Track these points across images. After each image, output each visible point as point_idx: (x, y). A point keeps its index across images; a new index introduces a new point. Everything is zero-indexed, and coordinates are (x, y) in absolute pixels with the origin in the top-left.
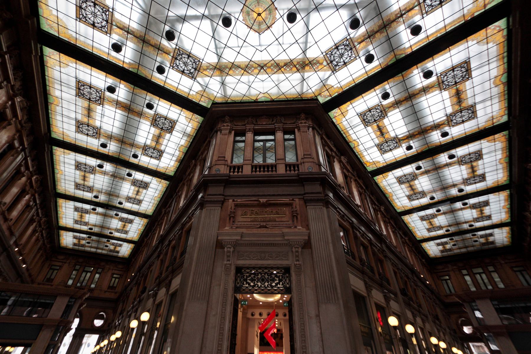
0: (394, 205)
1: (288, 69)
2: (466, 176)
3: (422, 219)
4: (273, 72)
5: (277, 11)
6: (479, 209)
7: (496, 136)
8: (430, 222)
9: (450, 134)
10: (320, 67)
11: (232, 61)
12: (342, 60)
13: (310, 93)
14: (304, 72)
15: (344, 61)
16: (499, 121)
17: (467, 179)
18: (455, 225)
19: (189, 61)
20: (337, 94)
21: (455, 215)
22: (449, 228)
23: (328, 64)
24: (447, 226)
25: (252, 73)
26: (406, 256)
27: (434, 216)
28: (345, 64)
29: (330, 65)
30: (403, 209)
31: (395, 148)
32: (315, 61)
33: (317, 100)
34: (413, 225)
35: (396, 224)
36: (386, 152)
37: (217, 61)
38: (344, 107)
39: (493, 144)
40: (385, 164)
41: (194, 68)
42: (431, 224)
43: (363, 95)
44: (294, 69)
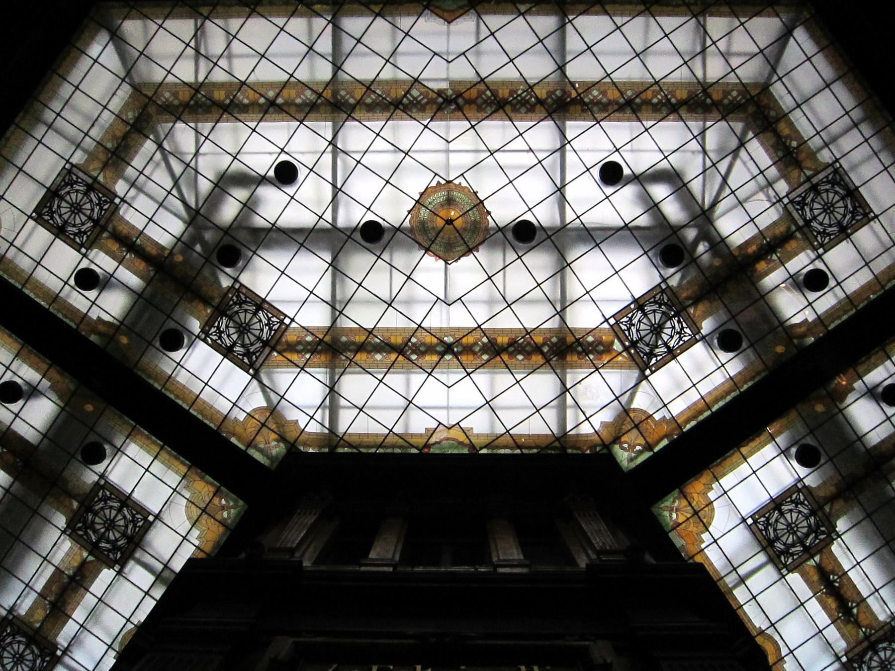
1: (520, 357)
4: (478, 362)
5: (489, 218)
11: (369, 325)
12: (660, 342)
13: (587, 435)
14: (564, 368)
15: (666, 344)
20: (665, 442)
23: (626, 349)
25: (420, 362)
28: (672, 354)
29: (633, 351)
32: (590, 339)
33: (611, 459)
37: (329, 325)
38: (695, 488)
41: (260, 342)
43: (744, 450)
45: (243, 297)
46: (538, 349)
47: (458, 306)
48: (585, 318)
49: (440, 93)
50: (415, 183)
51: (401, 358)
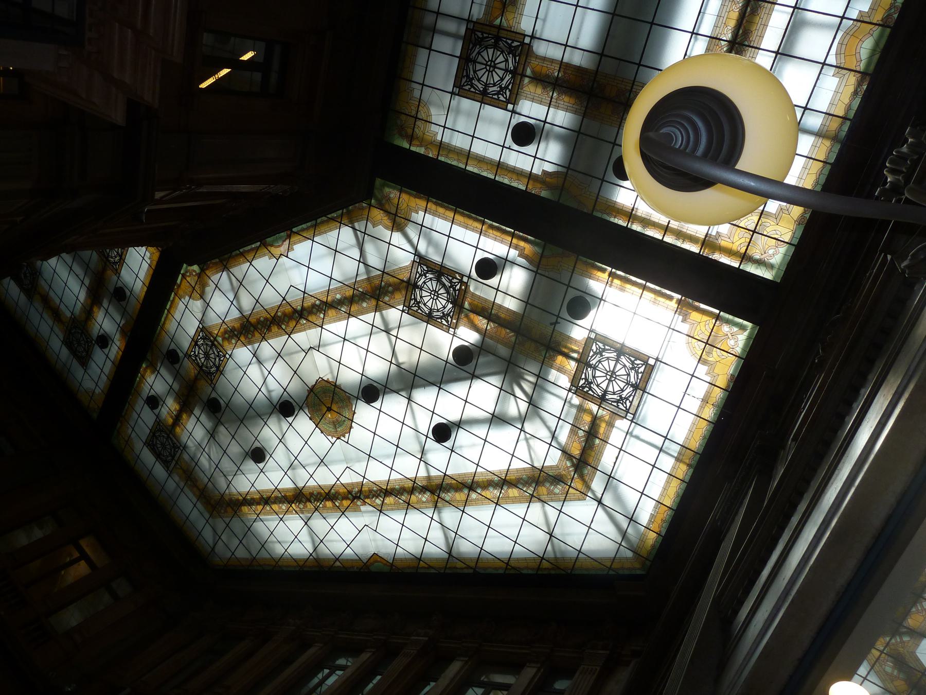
4: (281, 309)
10: (222, 330)
11: (352, 320)
19: (429, 304)
20: (178, 282)
23: (215, 339)
32: (233, 341)
44: (253, 320)
45: (444, 322)
46: (256, 328)
47: (306, 347)
48: (242, 354)
49: (365, 503)
50: (358, 435)
51: (325, 299)
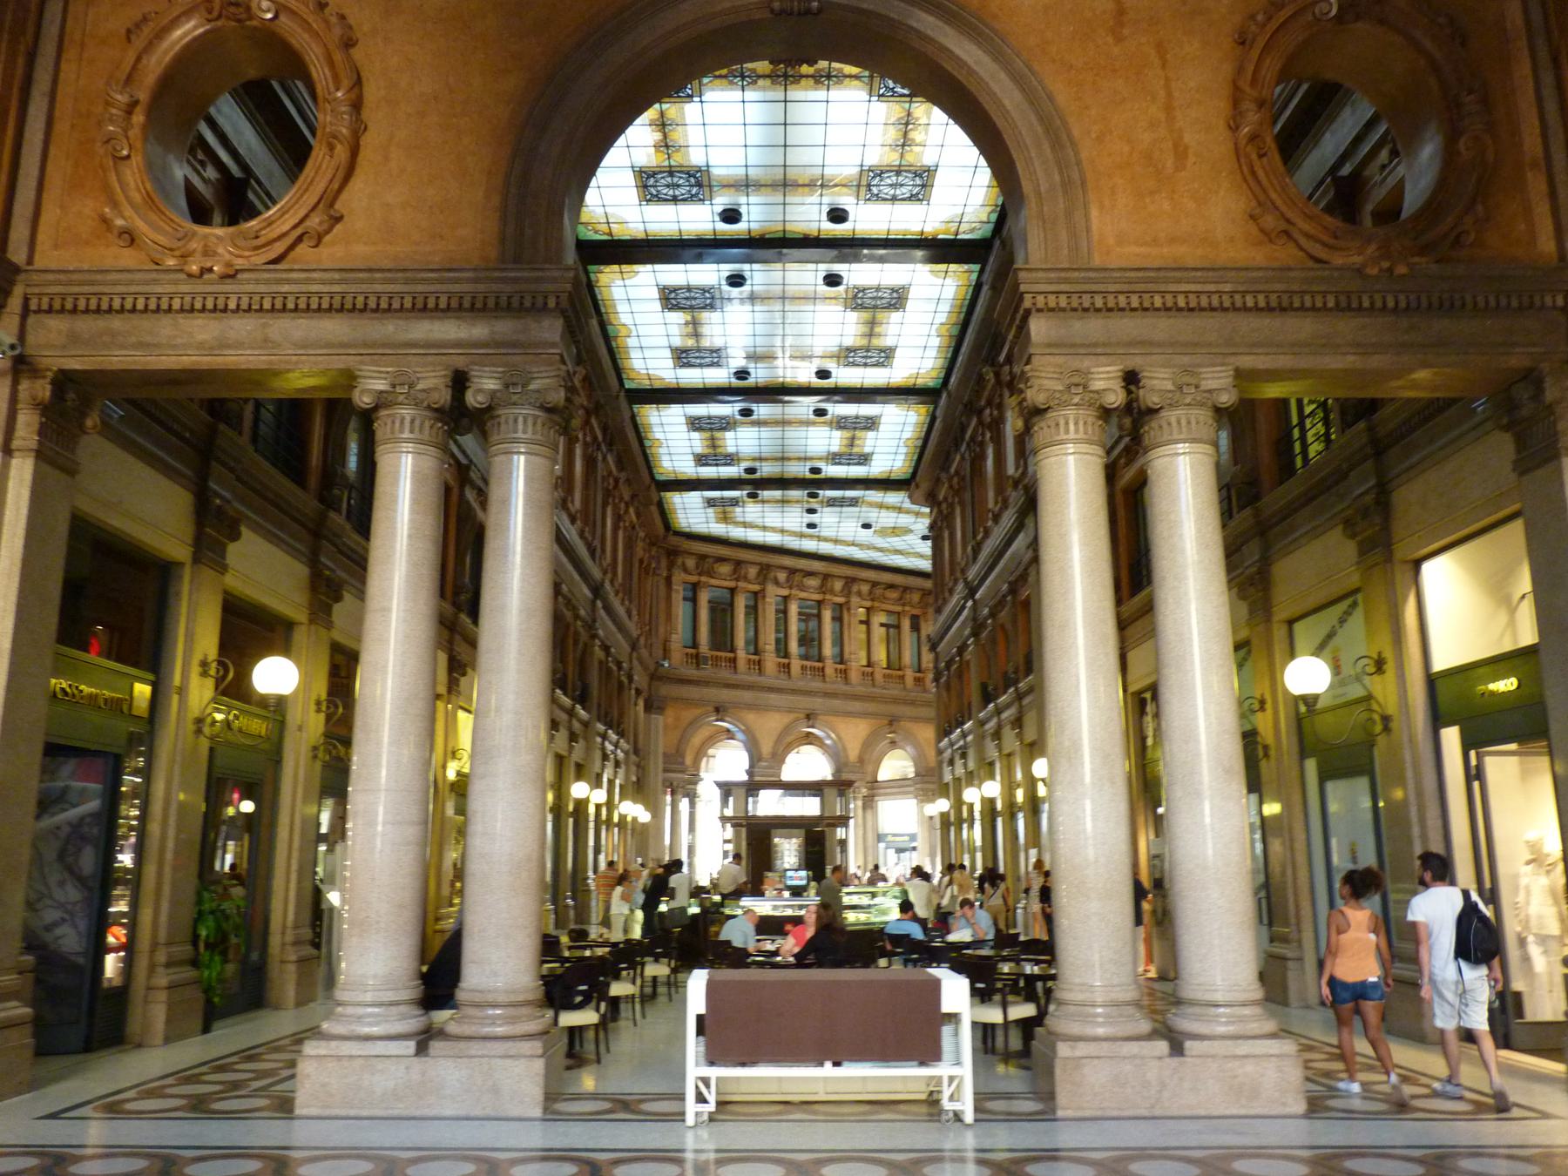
0: (624, 364)
2: (849, 342)
3: (695, 424)
6: (847, 434)
7: (953, 267)
8: (713, 439)
9: (851, 217)
16: (972, 231)
17: (849, 350)
18: (776, 459)
21: (787, 435)
22: (757, 464)
24: (754, 459)
26: (597, 543)
27: (726, 424)
30: (646, 384)
31: (691, 199)
34: (658, 436)
35: (605, 429)
36: (658, 199)
39: (940, 281)
40: (641, 236)
42: (714, 447)
